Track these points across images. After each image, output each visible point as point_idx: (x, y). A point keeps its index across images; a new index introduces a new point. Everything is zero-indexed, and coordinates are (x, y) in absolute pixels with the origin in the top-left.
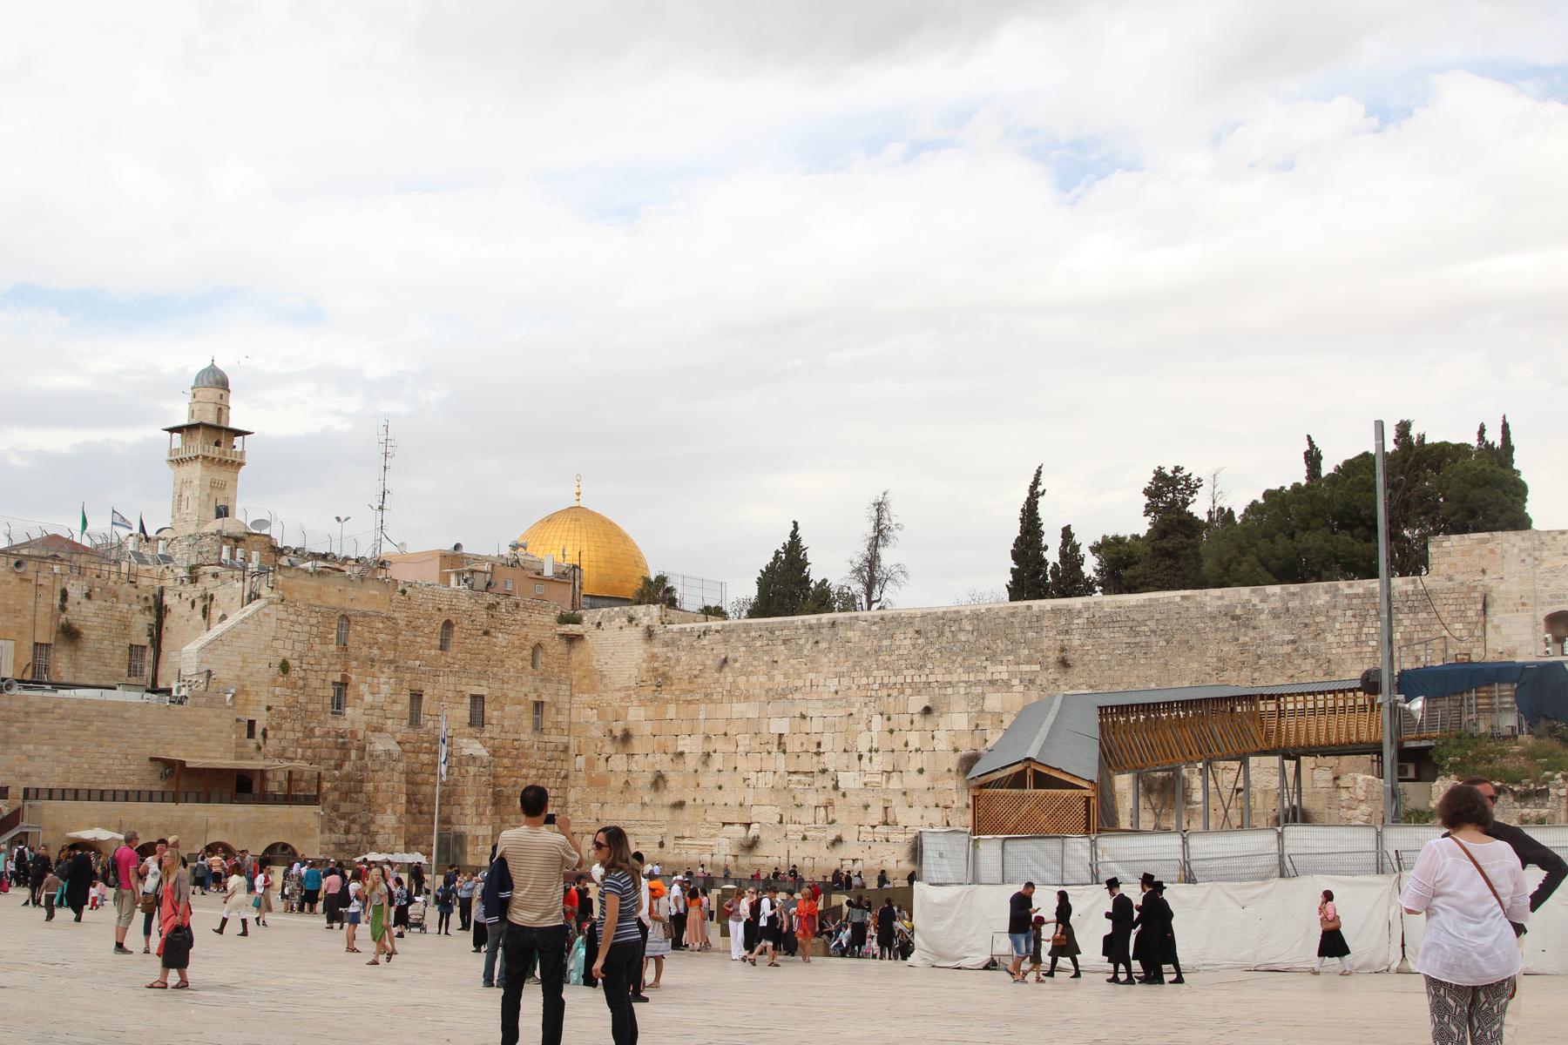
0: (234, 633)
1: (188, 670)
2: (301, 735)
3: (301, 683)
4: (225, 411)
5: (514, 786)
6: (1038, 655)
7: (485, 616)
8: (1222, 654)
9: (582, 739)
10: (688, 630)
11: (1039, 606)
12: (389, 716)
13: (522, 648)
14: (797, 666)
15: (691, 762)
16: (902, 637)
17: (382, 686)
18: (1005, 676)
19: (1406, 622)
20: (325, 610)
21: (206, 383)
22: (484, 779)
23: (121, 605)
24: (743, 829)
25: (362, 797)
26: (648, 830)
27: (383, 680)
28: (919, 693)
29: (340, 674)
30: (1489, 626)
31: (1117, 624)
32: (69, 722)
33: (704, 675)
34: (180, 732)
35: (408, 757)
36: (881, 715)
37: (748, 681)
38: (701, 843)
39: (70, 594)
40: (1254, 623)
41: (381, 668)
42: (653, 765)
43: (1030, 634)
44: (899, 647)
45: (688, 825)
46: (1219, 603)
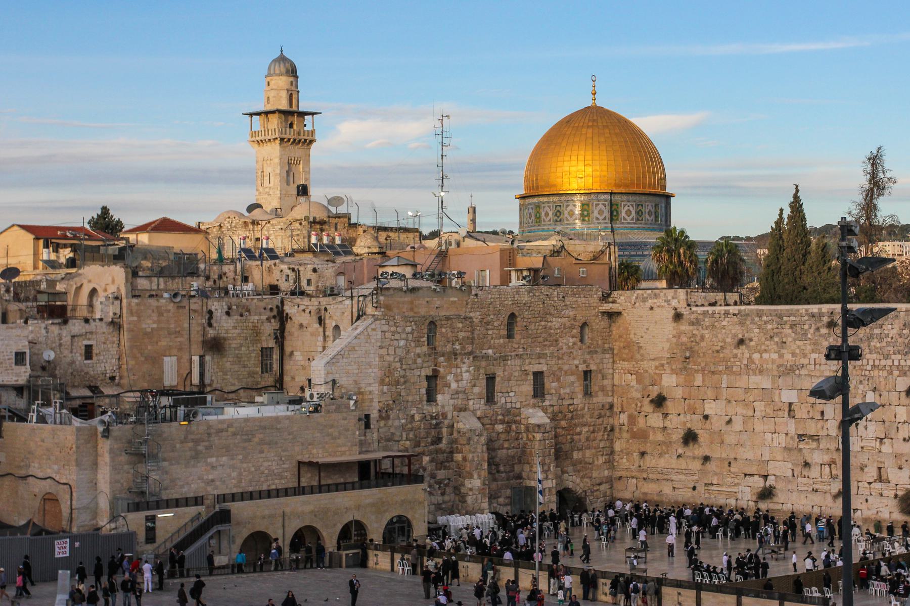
0: (351, 348)
1: (317, 380)
2: (403, 421)
3: (402, 380)
5: (571, 443)
7: (541, 306)
9: (624, 399)
10: (710, 312)
12: (470, 397)
13: (572, 327)
14: (803, 347)
15: (717, 423)
20: (417, 319)
21: (277, 72)
23: (252, 317)
24: (761, 480)
25: (453, 465)
26: (683, 477)
27: (464, 368)
29: (431, 369)
32: (238, 437)
33: (724, 351)
35: (487, 429)
36: (874, 391)
37: (761, 357)
38: (726, 490)
39: (214, 314)
41: (462, 359)
42: (685, 423)
44: (887, 336)
45: (716, 474)
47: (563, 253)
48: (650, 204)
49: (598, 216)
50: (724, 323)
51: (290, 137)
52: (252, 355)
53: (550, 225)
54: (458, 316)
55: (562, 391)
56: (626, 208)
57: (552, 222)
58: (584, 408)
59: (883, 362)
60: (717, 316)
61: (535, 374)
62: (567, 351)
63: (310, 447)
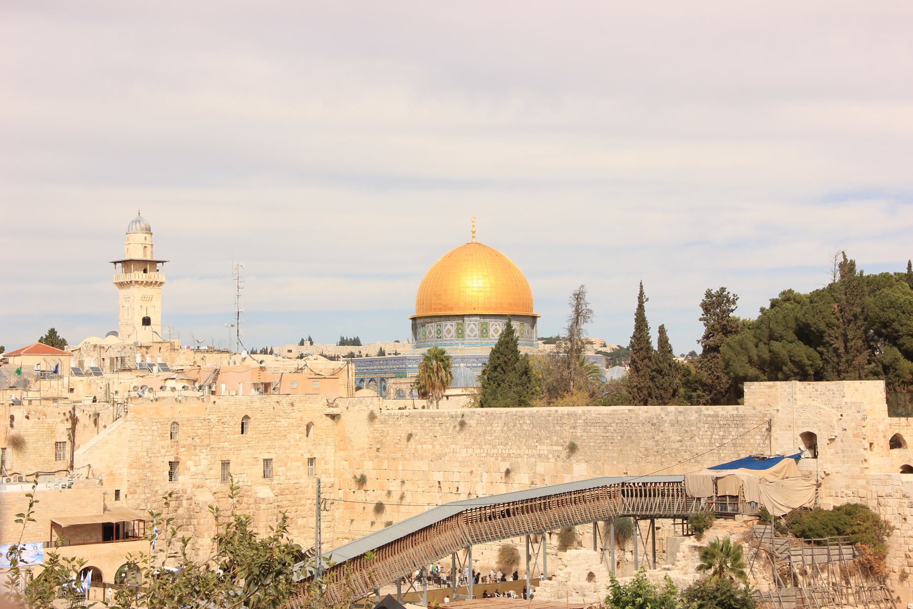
2: (149, 495)
3: (148, 465)
4: (149, 247)
6: (561, 441)
7: (272, 410)
9: (341, 479)
12: (207, 478)
13: (299, 426)
16: (496, 425)
17: (202, 461)
18: (546, 452)
19: (733, 433)
21: (134, 230)
22: (270, 511)
25: (191, 528)
27: (203, 456)
28: (504, 460)
29: (173, 456)
30: (772, 438)
39: (15, 418)
40: (662, 428)
41: (200, 450)
43: (558, 428)
46: (646, 415)
47: (306, 371)
49: (470, 334)
50: (401, 422)
51: (143, 280)
52: (48, 447)
55: (288, 473)
56: (494, 327)
60: (396, 417)
61: (264, 460)
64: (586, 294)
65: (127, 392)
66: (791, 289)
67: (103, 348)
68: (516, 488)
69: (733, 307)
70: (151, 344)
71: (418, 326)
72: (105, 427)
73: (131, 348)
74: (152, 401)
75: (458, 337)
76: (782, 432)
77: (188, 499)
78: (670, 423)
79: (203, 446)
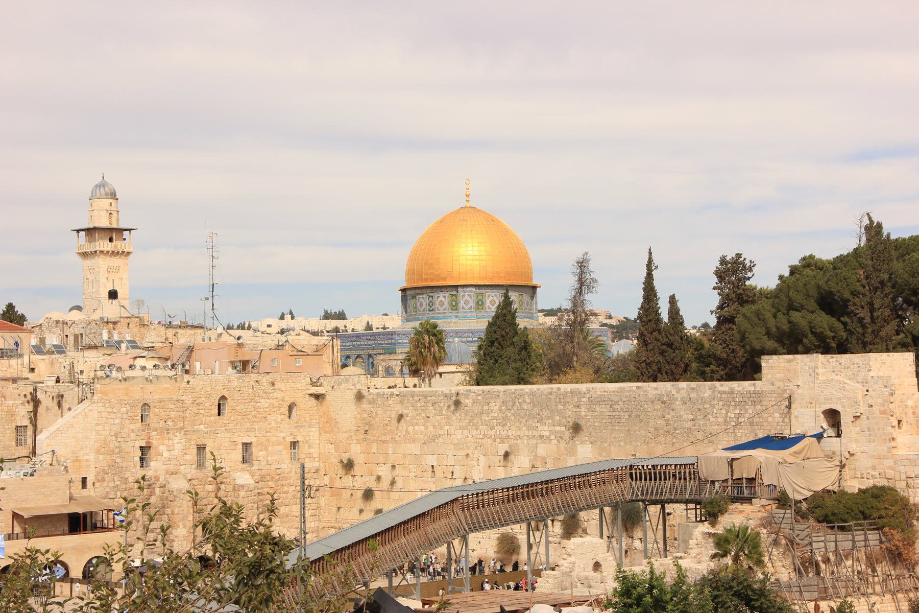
3: (117, 450)
4: (115, 214)
6: (564, 421)
7: (251, 390)
8: (657, 426)
11: (564, 389)
13: (280, 407)
14: (440, 421)
17: (176, 445)
18: (547, 434)
19: (750, 411)
22: (250, 498)
23: (7, 402)
25: (165, 517)
27: (176, 440)
28: (502, 442)
30: (792, 416)
31: (603, 403)
34: (32, 493)
40: (673, 406)
43: (560, 407)
46: (656, 392)
47: (287, 347)
48: (514, 294)
49: (464, 306)
53: (424, 314)
54: (171, 400)
56: (491, 298)
57: (425, 312)
58: (291, 472)
59: (490, 432)
60: (386, 396)
61: (243, 444)
62: (275, 426)
63: (23, 503)
64: (591, 262)
65: (93, 372)
66: (811, 255)
67: (67, 323)
68: (515, 471)
69: (749, 275)
70: (119, 320)
71: (408, 298)
72: (70, 409)
73: (96, 324)
74: (120, 380)
75: (452, 309)
76: (802, 410)
77: (161, 487)
78: (681, 400)
79: (177, 429)
